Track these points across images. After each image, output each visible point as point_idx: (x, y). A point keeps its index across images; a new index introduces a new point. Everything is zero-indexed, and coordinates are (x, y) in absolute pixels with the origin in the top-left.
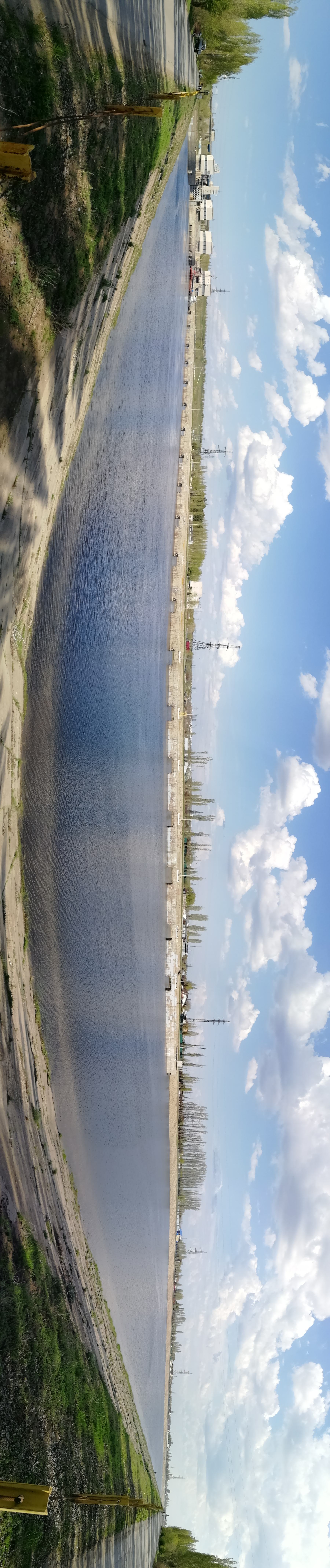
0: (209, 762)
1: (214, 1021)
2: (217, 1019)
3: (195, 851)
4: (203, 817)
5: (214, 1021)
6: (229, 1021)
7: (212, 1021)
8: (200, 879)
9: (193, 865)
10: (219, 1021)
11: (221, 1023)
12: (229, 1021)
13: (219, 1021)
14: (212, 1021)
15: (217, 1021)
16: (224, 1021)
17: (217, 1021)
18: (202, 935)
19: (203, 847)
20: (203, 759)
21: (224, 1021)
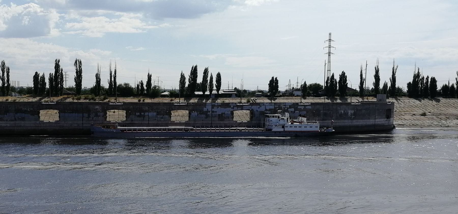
0: (7, 65)
1: (329, 54)
2: (327, 50)
3: (118, 84)
4: (77, 72)
5: (329, 54)
6: (330, 34)
7: (329, 55)
8: (150, 77)
9: (133, 85)
10: (330, 47)
11: (332, 44)
12: (330, 34)
13: (330, 47)
14: (329, 55)
15: (330, 50)
16: (330, 40)
17: (330, 50)
18: (213, 72)
19: (113, 73)
20: (3, 73)
21: (330, 40)
